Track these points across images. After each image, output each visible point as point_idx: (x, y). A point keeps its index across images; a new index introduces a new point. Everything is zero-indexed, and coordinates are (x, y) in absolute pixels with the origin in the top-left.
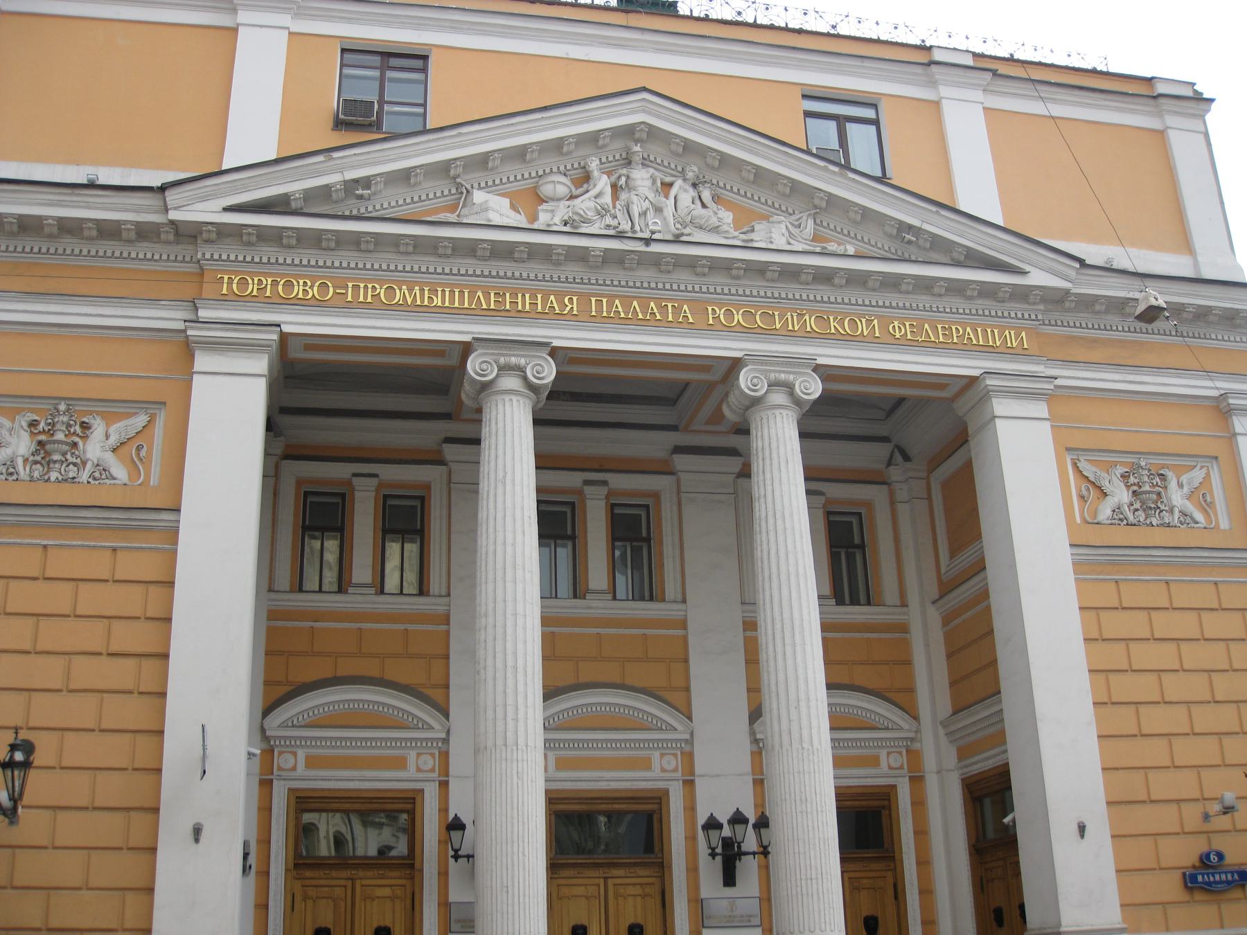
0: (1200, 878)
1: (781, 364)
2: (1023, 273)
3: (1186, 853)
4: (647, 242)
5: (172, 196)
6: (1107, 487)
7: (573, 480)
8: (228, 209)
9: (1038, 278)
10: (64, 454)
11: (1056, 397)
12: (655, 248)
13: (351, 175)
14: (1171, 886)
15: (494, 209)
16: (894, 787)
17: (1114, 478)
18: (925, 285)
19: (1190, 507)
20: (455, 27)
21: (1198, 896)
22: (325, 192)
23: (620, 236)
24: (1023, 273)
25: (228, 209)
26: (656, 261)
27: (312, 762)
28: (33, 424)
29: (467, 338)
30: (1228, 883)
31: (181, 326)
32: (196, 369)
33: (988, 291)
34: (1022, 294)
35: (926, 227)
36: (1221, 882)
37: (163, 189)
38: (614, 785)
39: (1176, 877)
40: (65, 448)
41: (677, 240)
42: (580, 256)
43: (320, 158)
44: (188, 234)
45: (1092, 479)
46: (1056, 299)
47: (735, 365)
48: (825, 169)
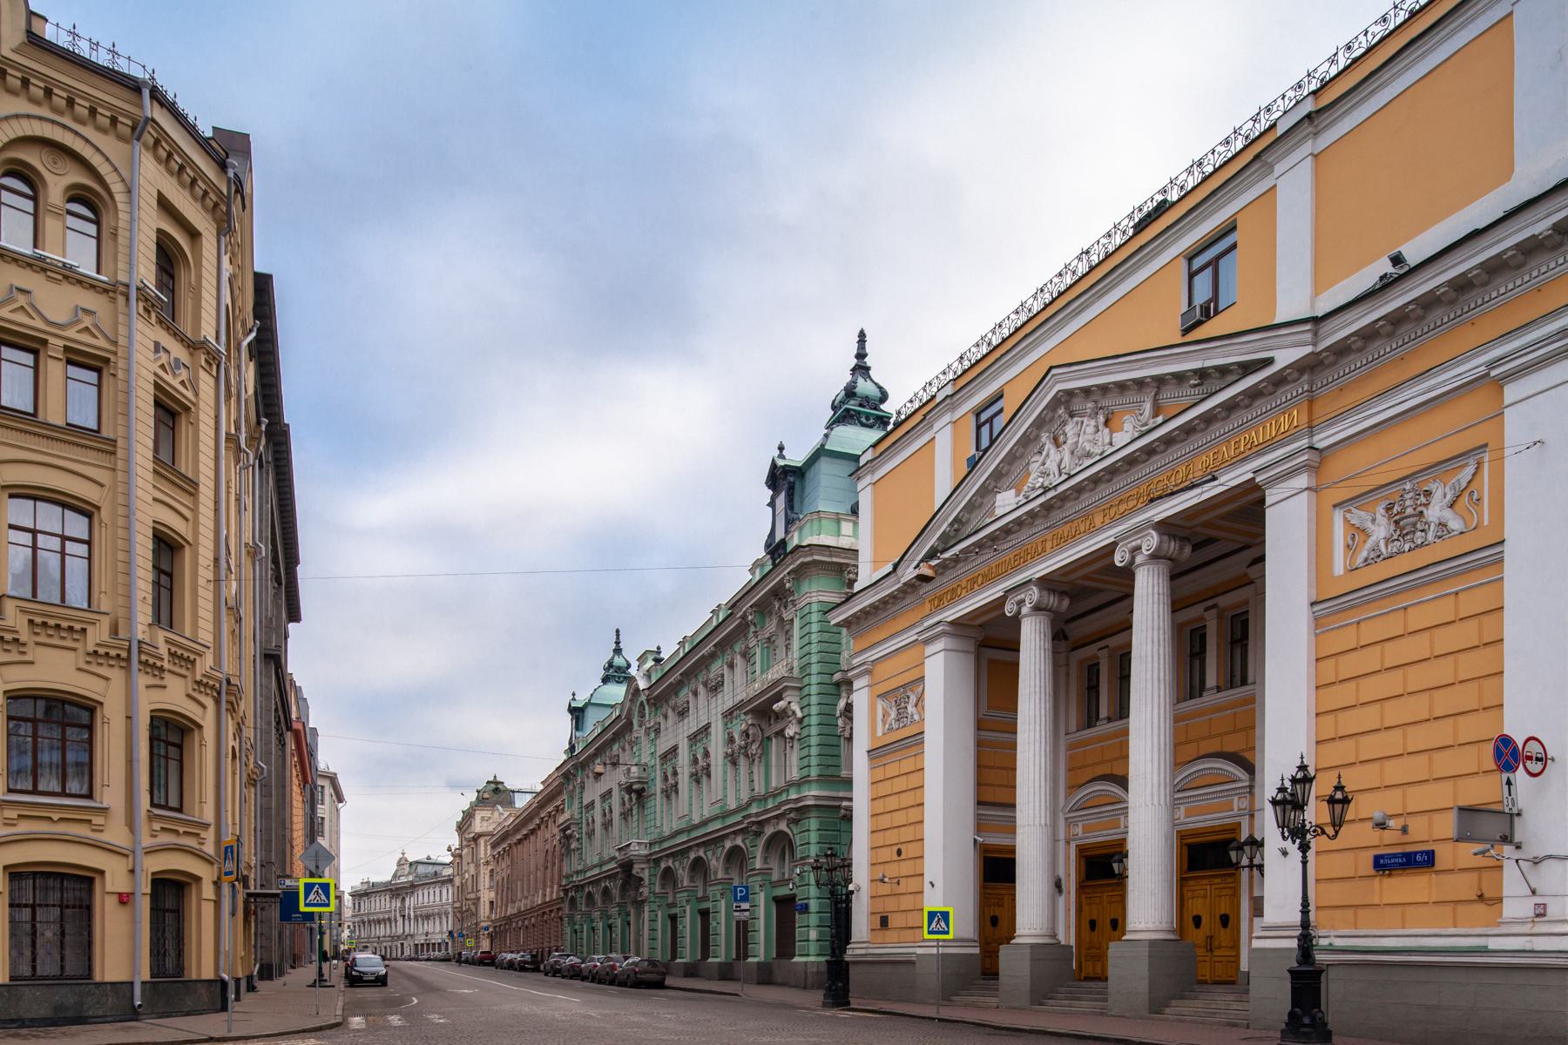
12: (1061, 489)
15: (1006, 502)
17: (1378, 516)
18: (1230, 407)
23: (1046, 490)
26: (1063, 498)
35: (1208, 364)
41: (1070, 477)
42: (1032, 515)
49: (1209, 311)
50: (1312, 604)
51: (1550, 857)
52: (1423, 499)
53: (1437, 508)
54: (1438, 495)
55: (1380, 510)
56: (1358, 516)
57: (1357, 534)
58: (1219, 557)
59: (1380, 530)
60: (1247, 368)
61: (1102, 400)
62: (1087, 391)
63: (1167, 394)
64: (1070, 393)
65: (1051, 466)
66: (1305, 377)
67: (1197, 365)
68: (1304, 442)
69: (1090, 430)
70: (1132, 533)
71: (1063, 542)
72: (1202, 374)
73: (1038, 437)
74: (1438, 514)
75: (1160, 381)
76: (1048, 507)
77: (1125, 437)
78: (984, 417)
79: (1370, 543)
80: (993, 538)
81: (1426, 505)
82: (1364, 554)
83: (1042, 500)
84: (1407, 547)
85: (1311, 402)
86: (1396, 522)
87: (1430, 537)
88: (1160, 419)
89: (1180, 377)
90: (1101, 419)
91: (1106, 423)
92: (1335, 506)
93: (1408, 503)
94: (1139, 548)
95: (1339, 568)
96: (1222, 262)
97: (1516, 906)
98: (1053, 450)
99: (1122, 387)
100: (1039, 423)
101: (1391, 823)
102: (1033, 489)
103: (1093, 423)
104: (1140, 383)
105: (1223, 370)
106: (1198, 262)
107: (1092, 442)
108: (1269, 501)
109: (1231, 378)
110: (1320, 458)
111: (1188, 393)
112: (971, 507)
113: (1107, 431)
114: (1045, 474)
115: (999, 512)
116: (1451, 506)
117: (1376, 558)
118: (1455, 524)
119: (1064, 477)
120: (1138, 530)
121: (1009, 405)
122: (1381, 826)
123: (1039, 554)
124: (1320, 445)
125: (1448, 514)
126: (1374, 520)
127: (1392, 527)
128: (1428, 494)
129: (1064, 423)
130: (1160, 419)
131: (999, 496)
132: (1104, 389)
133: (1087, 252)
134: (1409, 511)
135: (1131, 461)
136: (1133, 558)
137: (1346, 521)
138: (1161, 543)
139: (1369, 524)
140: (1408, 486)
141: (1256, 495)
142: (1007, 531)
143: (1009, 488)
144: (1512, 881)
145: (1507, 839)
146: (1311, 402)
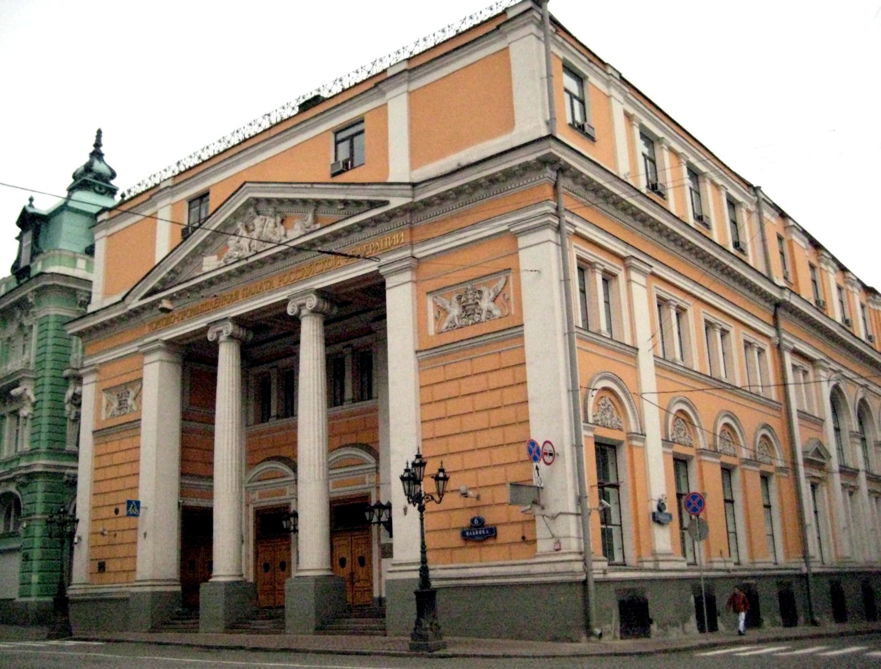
0: (467, 534)
2: (386, 203)
3: (463, 520)
4: (247, 259)
7: (339, 347)
8: (142, 298)
9: (396, 202)
10: (474, 310)
11: (416, 264)
12: (251, 260)
13: (169, 269)
14: (455, 539)
15: (210, 264)
18: (362, 225)
21: (470, 544)
22: (163, 282)
23: (239, 260)
24: (386, 203)
25: (142, 298)
26: (251, 267)
27: (261, 496)
28: (459, 298)
30: (482, 535)
31: (137, 349)
33: (376, 221)
34: (391, 215)
36: (479, 535)
37: (124, 299)
39: (458, 533)
40: (473, 307)
41: (257, 253)
42: (229, 275)
46: (409, 210)
49: (347, 166)
50: (417, 352)
52: (478, 295)
53: (486, 301)
54: (485, 294)
55: (454, 298)
56: (442, 301)
57: (441, 311)
58: (355, 318)
59: (455, 311)
60: (373, 205)
61: (282, 209)
65: (240, 246)
66: (408, 215)
67: (342, 197)
68: (407, 253)
70: (300, 293)
71: (250, 295)
72: (345, 203)
73: (234, 224)
75: (318, 203)
76: (241, 271)
77: (296, 232)
80: (200, 287)
81: (480, 299)
82: (446, 325)
83: (237, 265)
84: (470, 322)
85: (411, 229)
86: (464, 307)
87: (483, 317)
88: (318, 226)
89: (331, 203)
92: (428, 293)
93: (470, 296)
94: (304, 305)
95: (432, 330)
96: (356, 139)
97: (544, 545)
101: (470, 493)
102: (231, 257)
104: (305, 202)
105: (358, 203)
106: (341, 136)
108: (388, 285)
109: (362, 208)
110: (416, 264)
112: (184, 263)
113: (282, 228)
114: (239, 249)
115: (206, 269)
116: (494, 301)
117: (453, 327)
118: (497, 313)
119: (253, 253)
120: (305, 293)
121: (213, 202)
122: (465, 495)
123: (233, 299)
124: (419, 256)
125: (492, 306)
128: (480, 292)
129: (254, 218)
130: (318, 226)
131: (205, 259)
134: (470, 302)
136: (300, 311)
137: (435, 303)
138: (319, 302)
139: (448, 307)
141: (379, 280)
142: (210, 283)
143: (212, 254)
145: (535, 502)
146: (411, 229)
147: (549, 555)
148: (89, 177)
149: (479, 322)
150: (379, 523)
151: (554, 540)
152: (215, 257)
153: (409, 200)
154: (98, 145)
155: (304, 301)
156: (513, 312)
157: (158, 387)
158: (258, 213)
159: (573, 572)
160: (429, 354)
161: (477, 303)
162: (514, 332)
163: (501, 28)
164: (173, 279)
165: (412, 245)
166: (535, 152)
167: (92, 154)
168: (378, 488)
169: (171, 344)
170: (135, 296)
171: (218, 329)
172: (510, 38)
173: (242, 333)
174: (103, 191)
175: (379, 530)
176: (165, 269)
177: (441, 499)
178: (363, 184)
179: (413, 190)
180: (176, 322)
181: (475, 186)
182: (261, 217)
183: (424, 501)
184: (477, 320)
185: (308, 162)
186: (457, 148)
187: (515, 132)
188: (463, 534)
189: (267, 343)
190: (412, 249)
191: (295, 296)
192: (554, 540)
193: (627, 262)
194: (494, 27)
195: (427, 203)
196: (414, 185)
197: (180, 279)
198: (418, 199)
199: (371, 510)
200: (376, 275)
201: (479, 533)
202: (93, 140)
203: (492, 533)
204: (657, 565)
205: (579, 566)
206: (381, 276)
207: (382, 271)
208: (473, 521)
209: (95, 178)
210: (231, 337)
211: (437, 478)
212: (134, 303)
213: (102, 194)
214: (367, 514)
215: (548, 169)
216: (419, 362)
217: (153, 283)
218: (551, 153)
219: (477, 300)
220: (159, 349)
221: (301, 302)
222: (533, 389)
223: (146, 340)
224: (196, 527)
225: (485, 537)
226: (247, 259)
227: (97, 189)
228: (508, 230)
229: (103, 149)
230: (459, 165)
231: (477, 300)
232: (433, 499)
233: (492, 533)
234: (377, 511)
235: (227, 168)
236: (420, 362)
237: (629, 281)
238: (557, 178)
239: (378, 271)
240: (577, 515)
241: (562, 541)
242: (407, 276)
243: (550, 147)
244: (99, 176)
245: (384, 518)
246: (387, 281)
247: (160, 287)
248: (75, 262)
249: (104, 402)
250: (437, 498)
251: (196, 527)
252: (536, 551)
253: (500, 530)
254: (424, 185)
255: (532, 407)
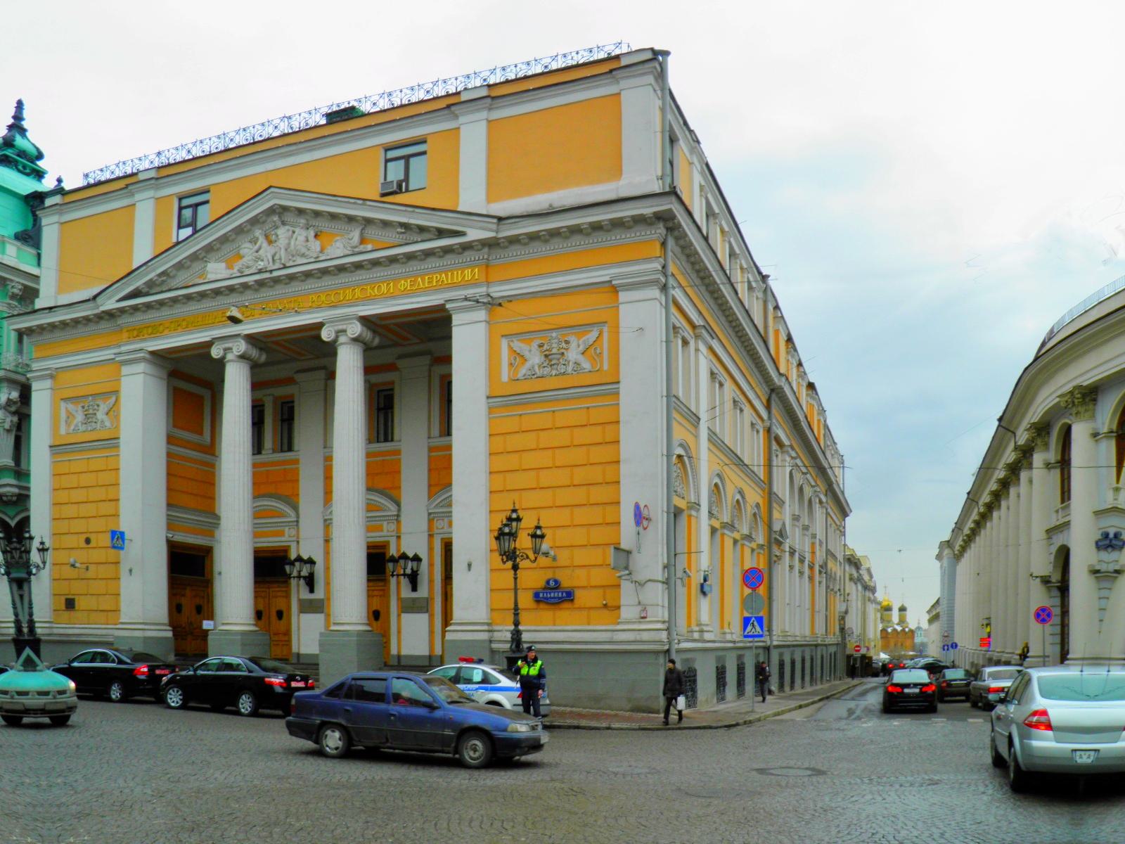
0: (541, 595)
1: (340, 319)
2: (462, 234)
4: (271, 271)
5: (99, 300)
6: (527, 354)
8: (119, 300)
9: (474, 234)
11: (493, 304)
12: (275, 274)
15: (217, 271)
16: (289, 546)
17: (533, 349)
19: (581, 358)
20: (218, 172)
21: (542, 606)
22: (150, 284)
23: (260, 271)
24: (462, 234)
25: (119, 300)
26: (276, 281)
29: (207, 339)
30: (559, 598)
32: (123, 373)
33: (447, 250)
34: (466, 247)
35: (412, 221)
36: (554, 598)
37: (95, 297)
38: (265, 545)
41: (285, 267)
43: (144, 267)
44: (110, 315)
45: (518, 352)
46: (491, 244)
47: (320, 326)
48: (354, 203)
50: (488, 397)
51: (650, 580)
52: (564, 345)
54: (573, 345)
55: (535, 344)
57: (518, 357)
58: (411, 353)
59: (535, 359)
60: (441, 233)
62: (301, 212)
63: (371, 232)
64: (285, 209)
65: (258, 256)
66: (486, 250)
67: (404, 220)
68: (483, 290)
69: (302, 238)
70: (340, 319)
71: (266, 312)
74: (575, 356)
75: (368, 222)
76: (261, 284)
77: (339, 249)
78: (185, 202)
79: (528, 365)
80: (203, 295)
81: (567, 349)
84: (554, 372)
85: (487, 266)
86: (546, 356)
89: (386, 224)
90: (312, 233)
91: (316, 236)
92: (502, 336)
93: (554, 345)
94: (344, 331)
95: (505, 377)
98: (265, 245)
99: (334, 217)
100: (254, 221)
102: (248, 267)
103: (304, 233)
105: (422, 229)
107: (295, 246)
108: (454, 323)
109: (426, 236)
110: (493, 304)
111: (391, 236)
112: (180, 266)
113: (318, 243)
115: (211, 277)
117: (532, 376)
118: (586, 365)
119: (277, 266)
120: (346, 318)
124: (494, 295)
126: (530, 351)
127: (543, 358)
128: (567, 342)
132: (317, 214)
133: (290, 118)
134: (554, 351)
135: (341, 269)
136: (337, 337)
138: (362, 331)
140: (554, 335)
141: (444, 314)
143: (217, 261)
144: (627, 594)
147: (634, 623)
148: (9, 152)
149: (564, 374)
150: (299, 577)
151: (639, 608)
152: (223, 265)
153: (492, 234)
154: (18, 117)
155: (344, 327)
156: (606, 367)
157: (139, 403)
158: (284, 223)
159: (660, 641)
160: (502, 401)
161: (563, 354)
162: (609, 387)
163: (614, 73)
164: (163, 282)
165: (488, 283)
166: (652, 206)
167: (10, 127)
168: (399, 537)
169: (159, 357)
170: (110, 298)
171: (227, 345)
172: (623, 84)
173: (254, 353)
174: (28, 171)
175: (398, 583)
176: (154, 270)
177: (536, 558)
178: (434, 209)
179: (498, 225)
180: (166, 332)
181: (575, 230)
182: (287, 227)
183: (518, 560)
184: (562, 371)
185: (355, 174)
186: (549, 189)
187: (623, 182)
188: (536, 595)
189: (291, 367)
190: (488, 287)
191: (333, 321)
192: (639, 608)
193: (697, 331)
194: (607, 70)
195: (514, 241)
196: (500, 219)
197: (173, 284)
198: (501, 235)
199: (292, 563)
200: (441, 308)
201: (555, 595)
202: (12, 111)
203: (569, 596)
204: (701, 636)
205: (664, 635)
206: (446, 310)
207: (448, 306)
208: (548, 582)
209: (18, 155)
210: (243, 357)
211: (534, 536)
212: (110, 304)
213: (28, 175)
214: (287, 568)
215: (661, 225)
216: (490, 408)
217: (138, 283)
218: (670, 210)
219: (563, 351)
220: (144, 359)
221: (340, 327)
222: (625, 450)
223: (124, 349)
224: (189, 568)
225: (560, 601)
226: (271, 271)
227: (20, 167)
228: (611, 281)
229: (25, 124)
230: (551, 206)
231: (563, 351)
232: (528, 557)
233: (569, 596)
234: (297, 564)
235: (238, 167)
236: (491, 410)
237: (697, 350)
238: (666, 235)
239: (443, 305)
240: (663, 583)
241: (649, 609)
242: (481, 314)
243: (671, 203)
244: (22, 153)
245: (305, 573)
246: (454, 317)
247: (145, 290)
248: (4, 248)
249: (63, 415)
250: (532, 556)
251: (189, 568)
252: (619, 617)
253: (578, 594)
254: (513, 220)
255: (624, 468)
